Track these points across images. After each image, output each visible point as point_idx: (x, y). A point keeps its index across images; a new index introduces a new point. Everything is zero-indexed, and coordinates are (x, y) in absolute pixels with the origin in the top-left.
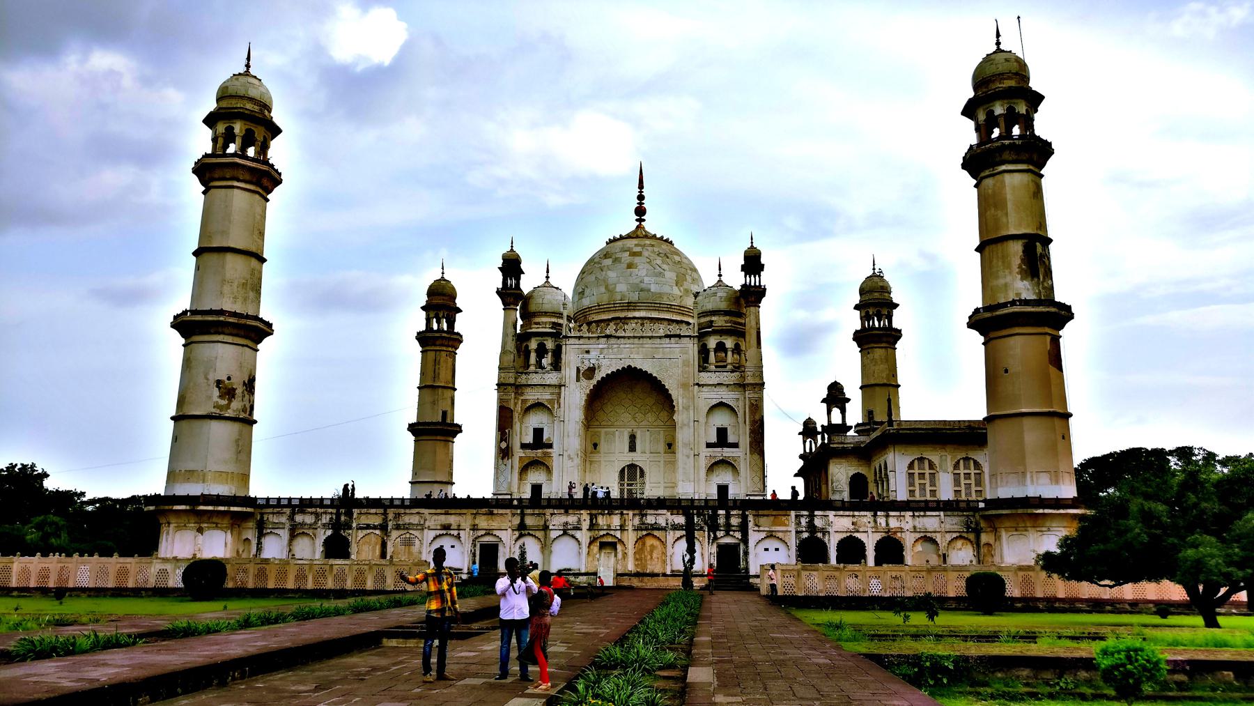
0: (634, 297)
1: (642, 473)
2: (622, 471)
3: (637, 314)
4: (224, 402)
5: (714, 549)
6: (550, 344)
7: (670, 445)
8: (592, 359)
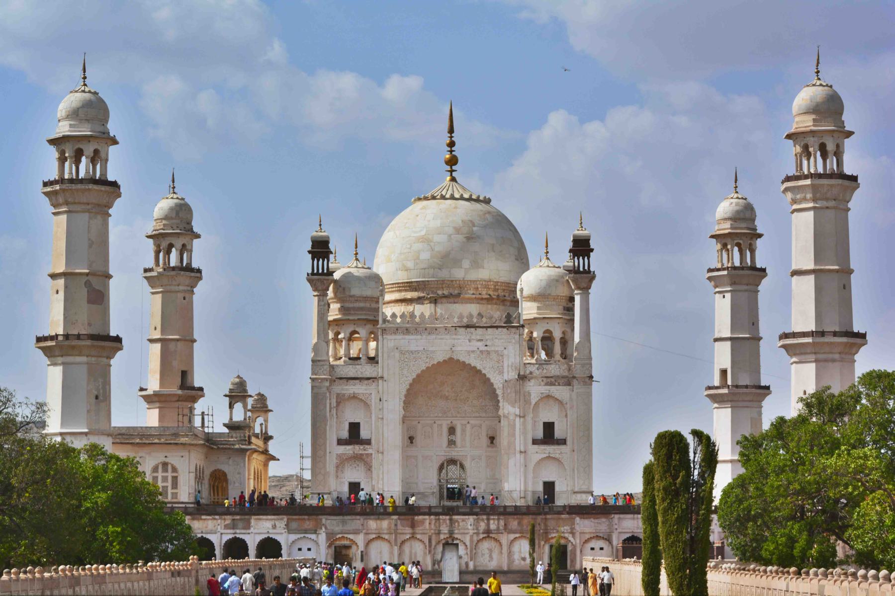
1: (462, 466)
2: (441, 468)
5: (547, 548)
6: (363, 332)
7: (492, 439)
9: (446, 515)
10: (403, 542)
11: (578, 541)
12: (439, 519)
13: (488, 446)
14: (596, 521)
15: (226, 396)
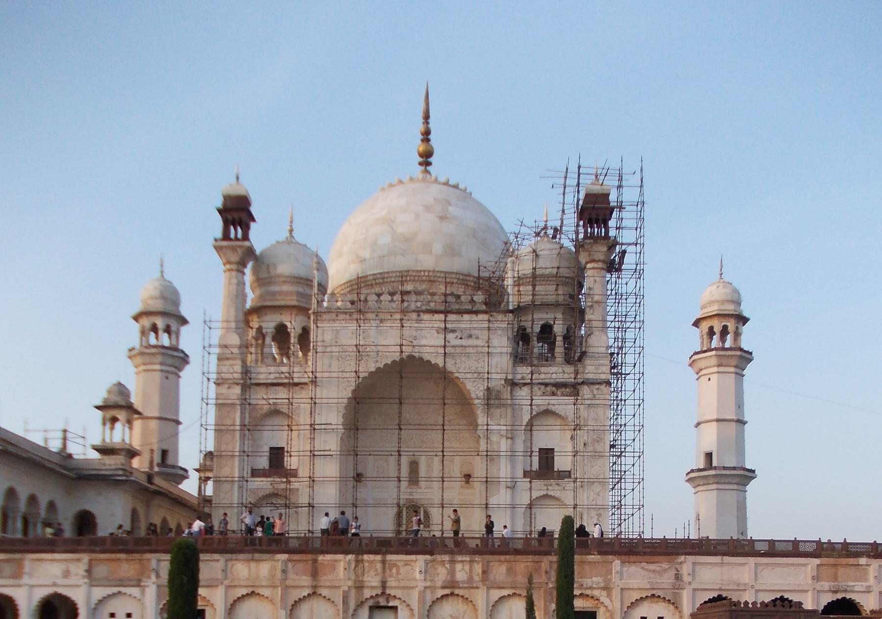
9: (376, 553)
10: (297, 603)
11: (618, 605)
12: (362, 560)
13: (462, 487)
14: (652, 567)
15: (98, 408)
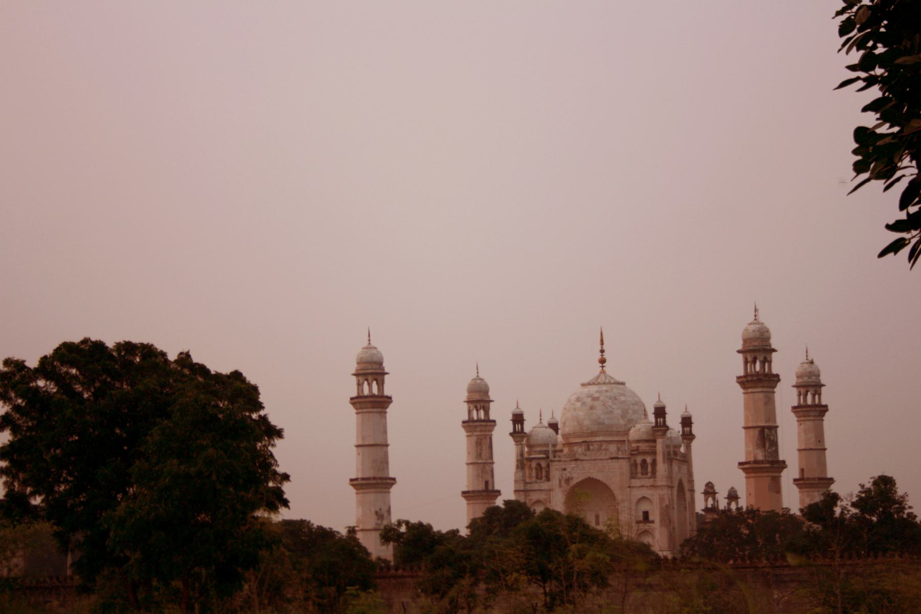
0: (595, 428)
3: (597, 439)
4: (379, 522)
8: (567, 474)
